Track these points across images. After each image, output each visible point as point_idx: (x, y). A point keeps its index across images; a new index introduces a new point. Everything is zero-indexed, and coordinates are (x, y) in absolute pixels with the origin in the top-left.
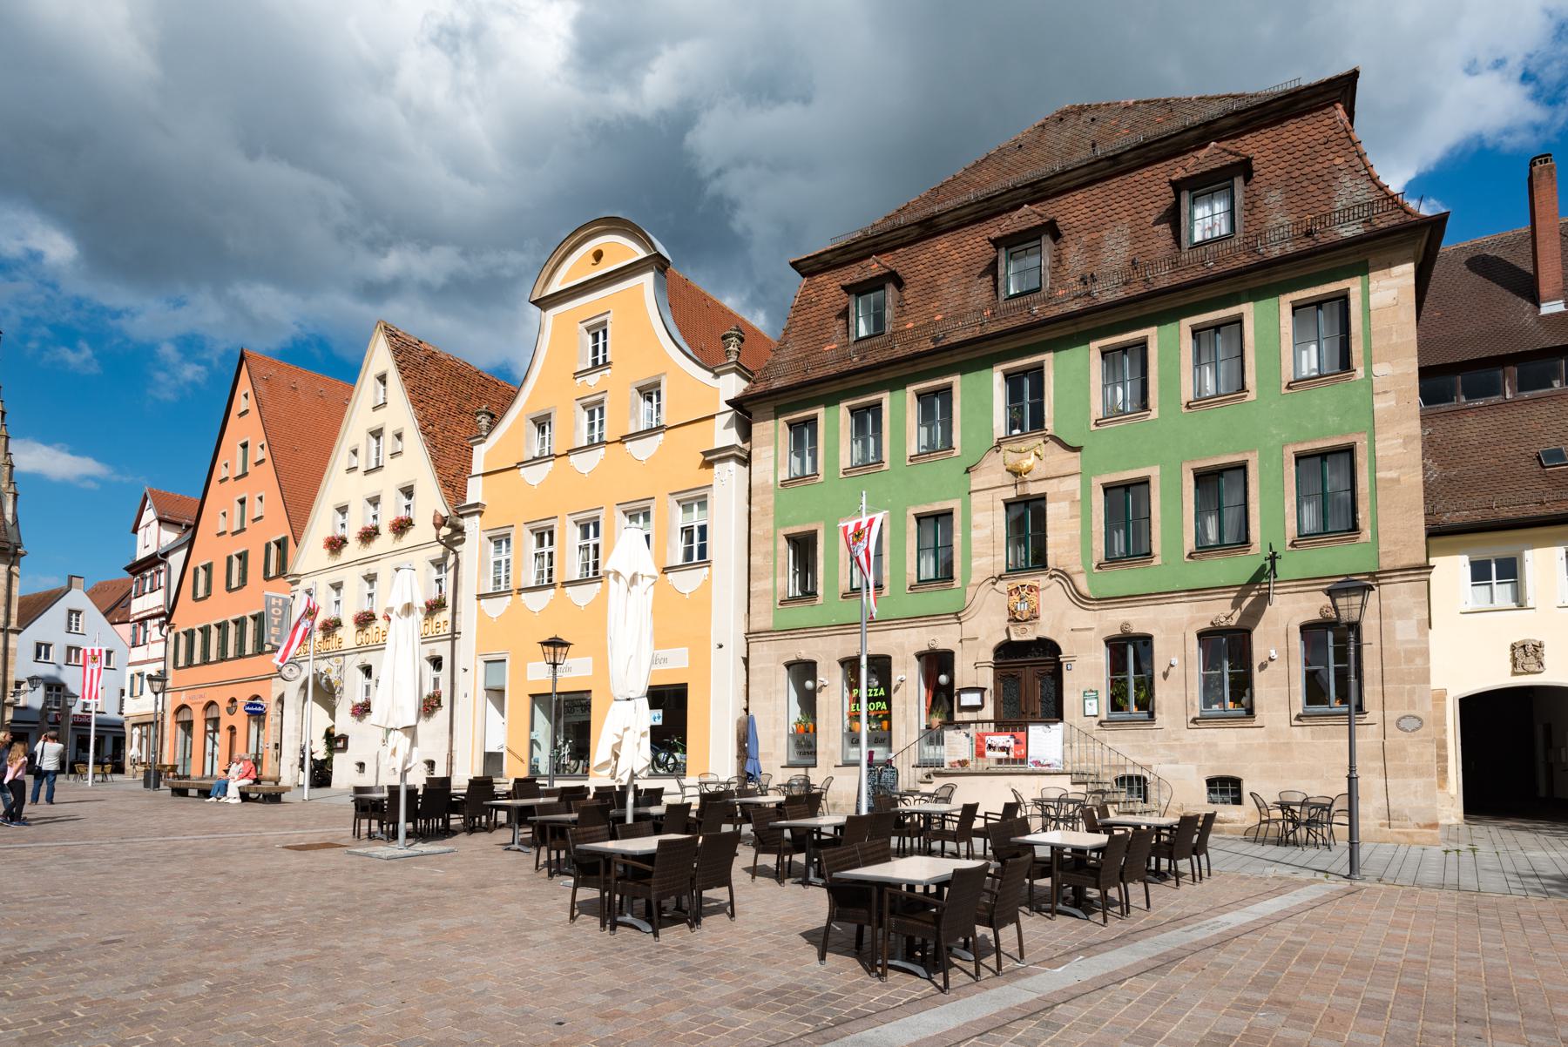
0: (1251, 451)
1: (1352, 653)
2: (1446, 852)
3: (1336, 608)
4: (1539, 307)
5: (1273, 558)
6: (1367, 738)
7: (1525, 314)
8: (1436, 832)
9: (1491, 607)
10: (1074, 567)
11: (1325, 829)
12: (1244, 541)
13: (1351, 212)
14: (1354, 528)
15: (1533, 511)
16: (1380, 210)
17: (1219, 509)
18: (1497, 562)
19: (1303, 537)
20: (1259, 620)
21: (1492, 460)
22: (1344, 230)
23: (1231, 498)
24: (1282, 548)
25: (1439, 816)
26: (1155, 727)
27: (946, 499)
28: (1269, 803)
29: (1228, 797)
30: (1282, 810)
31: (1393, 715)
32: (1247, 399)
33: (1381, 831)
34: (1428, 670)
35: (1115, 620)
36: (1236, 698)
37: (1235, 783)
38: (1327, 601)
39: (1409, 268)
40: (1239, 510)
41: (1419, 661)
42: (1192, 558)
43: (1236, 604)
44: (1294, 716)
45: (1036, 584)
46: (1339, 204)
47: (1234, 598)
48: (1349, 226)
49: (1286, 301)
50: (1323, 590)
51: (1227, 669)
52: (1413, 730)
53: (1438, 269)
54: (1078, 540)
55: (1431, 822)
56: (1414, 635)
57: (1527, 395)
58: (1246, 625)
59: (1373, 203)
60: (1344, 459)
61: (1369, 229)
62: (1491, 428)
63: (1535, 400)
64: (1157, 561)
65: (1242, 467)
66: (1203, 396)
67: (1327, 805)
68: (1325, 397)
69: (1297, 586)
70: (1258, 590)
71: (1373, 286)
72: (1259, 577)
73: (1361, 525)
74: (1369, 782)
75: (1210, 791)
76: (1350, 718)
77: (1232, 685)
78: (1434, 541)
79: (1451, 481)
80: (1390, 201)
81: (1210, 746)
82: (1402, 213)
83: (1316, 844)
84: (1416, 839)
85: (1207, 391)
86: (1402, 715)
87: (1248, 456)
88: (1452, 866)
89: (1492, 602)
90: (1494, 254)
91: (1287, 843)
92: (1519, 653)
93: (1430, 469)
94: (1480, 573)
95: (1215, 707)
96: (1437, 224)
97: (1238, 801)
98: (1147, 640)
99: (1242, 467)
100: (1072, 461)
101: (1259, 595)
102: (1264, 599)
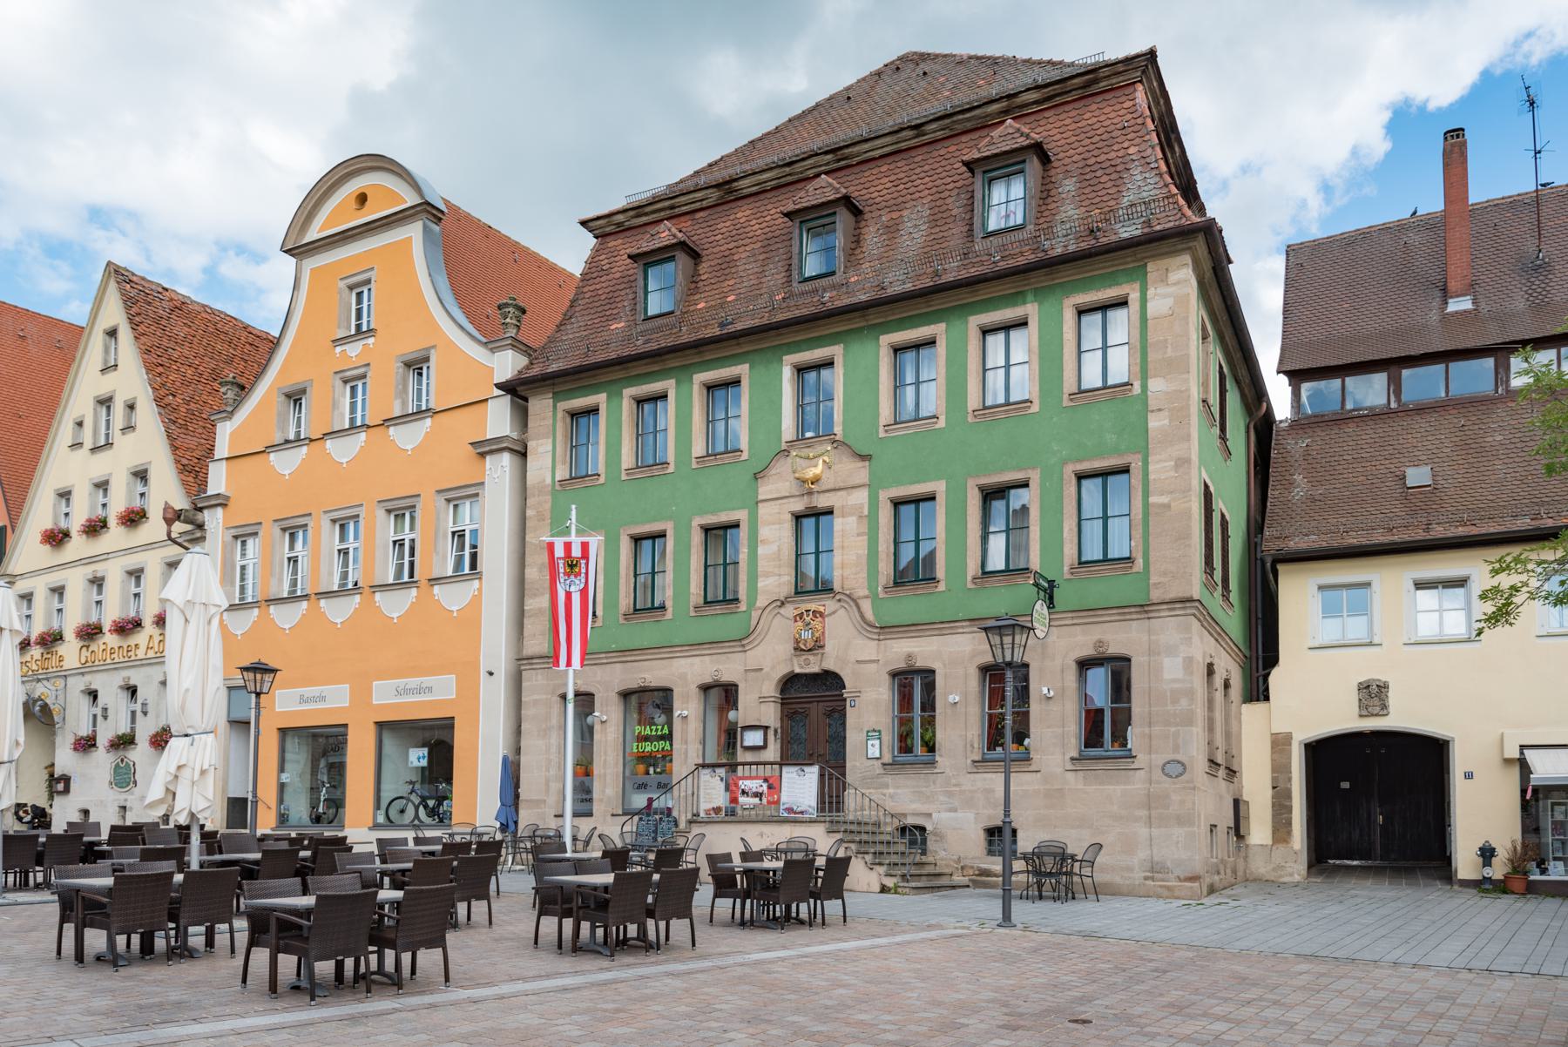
0: (1034, 468)
10: (862, 591)
26: (936, 771)
27: (733, 509)
35: (902, 650)
45: (822, 609)
54: (864, 561)
64: (942, 587)
95: (999, 749)
98: (930, 673)
100: (860, 472)
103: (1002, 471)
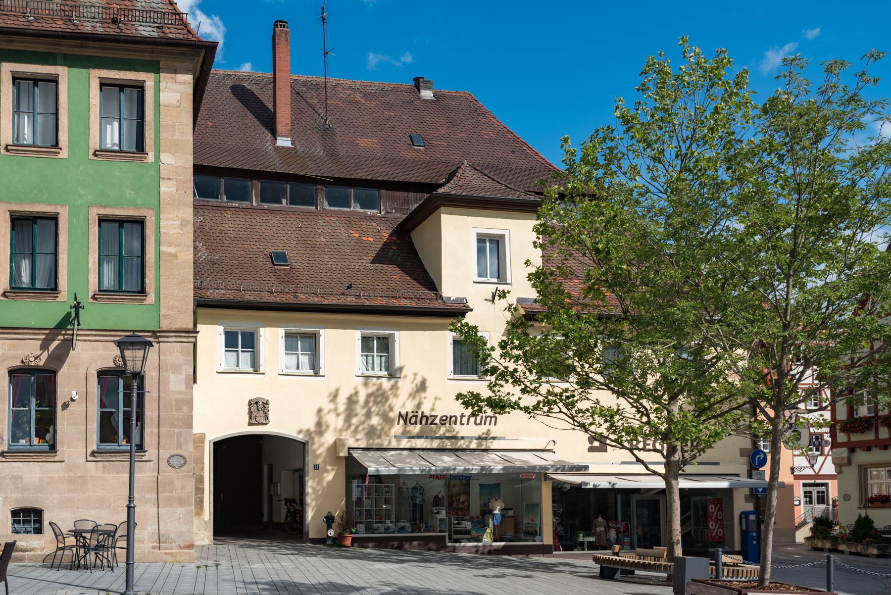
0: (62, 205)
1: (135, 399)
2: (198, 567)
3: (123, 358)
4: (276, 139)
5: (77, 307)
6: (145, 473)
7: (267, 142)
8: (192, 551)
9: (237, 369)
11: (110, 553)
12: (54, 289)
13: (148, 15)
14: (142, 291)
15: (266, 298)
16: (170, 22)
17: (32, 254)
18: (243, 334)
19: (102, 293)
20: (64, 363)
21: (242, 253)
22: (143, 28)
23: (43, 246)
24: (85, 299)
25: (195, 538)
28: (65, 531)
29: (32, 526)
30: (76, 538)
31: (165, 454)
32: (60, 156)
33: (153, 552)
34: (191, 417)
36: (41, 435)
37: (38, 513)
38: (117, 351)
39: (189, 78)
40: (50, 258)
41: (185, 409)
42: (6, 297)
43: (44, 347)
44: (89, 452)
46: (139, 4)
47: (43, 340)
48: (146, 26)
49: (96, 75)
50: (114, 341)
51: (34, 407)
52: (179, 467)
53: (210, 86)
55: (189, 544)
56: (183, 388)
57: (266, 206)
58: (52, 366)
59: (164, 13)
60: (137, 227)
61: (161, 34)
62: (242, 226)
63: (271, 211)
65: (54, 218)
66: (21, 142)
67: (112, 531)
68: (122, 170)
69: (96, 335)
70: (64, 335)
71: (163, 85)
72: (64, 323)
73: (147, 290)
74: (145, 511)
75: (15, 522)
76: (131, 456)
77: (38, 421)
78: (200, 311)
79: (214, 264)
80: (177, 17)
81: (16, 478)
82: (185, 31)
83: (102, 567)
84: (178, 558)
85: (25, 139)
86: (172, 454)
87: (59, 209)
88: (201, 579)
89: (238, 366)
90: (249, 87)
91: (78, 567)
92: (254, 408)
93: (200, 251)
94: (231, 341)
96: (210, 48)
97: (39, 531)
99: (54, 218)
101: (64, 340)
102: (68, 345)
103: (32, 203)
